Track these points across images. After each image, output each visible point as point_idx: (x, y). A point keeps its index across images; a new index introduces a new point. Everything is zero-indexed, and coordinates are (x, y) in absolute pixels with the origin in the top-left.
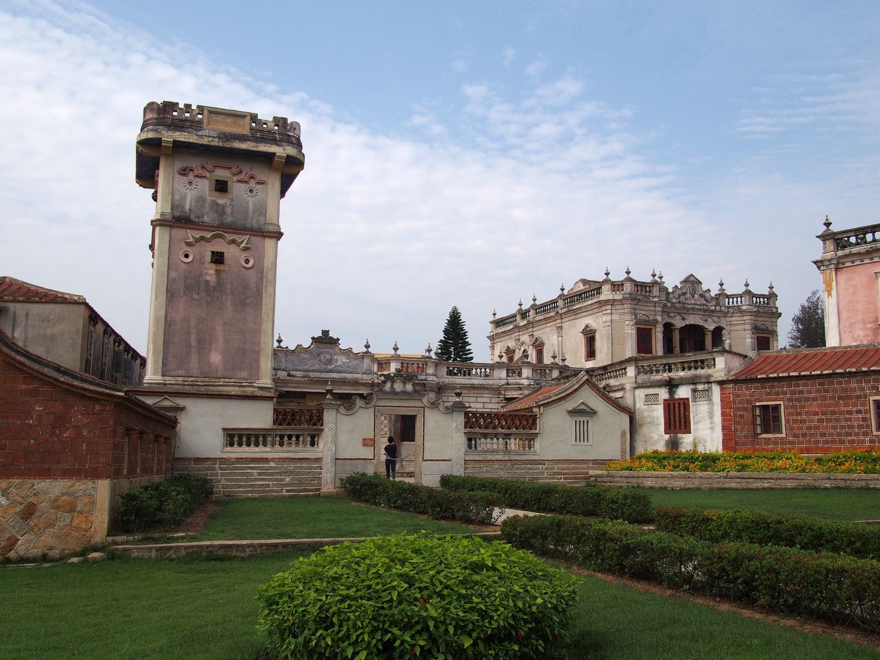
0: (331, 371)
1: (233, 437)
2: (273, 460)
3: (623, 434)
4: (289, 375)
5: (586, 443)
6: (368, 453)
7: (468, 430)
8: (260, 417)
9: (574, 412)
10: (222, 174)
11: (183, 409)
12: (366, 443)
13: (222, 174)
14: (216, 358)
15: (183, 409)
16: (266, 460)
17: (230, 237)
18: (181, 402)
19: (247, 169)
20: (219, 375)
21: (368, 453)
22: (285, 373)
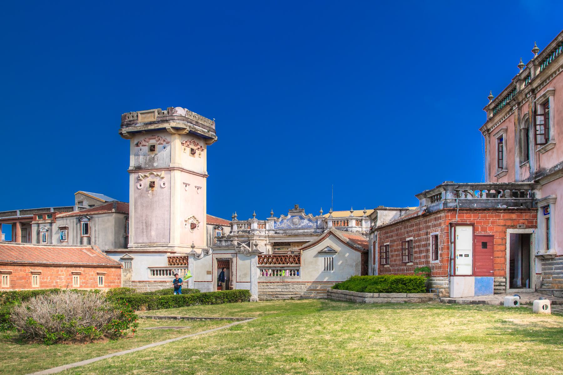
0: (300, 229)
1: (155, 271)
2: (168, 282)
3: (357, 265)
4: (276, 233)
5: (332, 272)
6: (209, 278)
7: (260, 265)
8: (162, 261)
9: (321, 253)
10: (153, 142)
11: (132, 259)
12: (208, 273)
13: (153, 142)
14: (153, 233)
15: (132, 259)
16: (165, 282)
17: (155, 173)
18: (132, 255)
19: (163, 136)
20: (155, 241)
21: (209, 278)
22: (273, 232)
